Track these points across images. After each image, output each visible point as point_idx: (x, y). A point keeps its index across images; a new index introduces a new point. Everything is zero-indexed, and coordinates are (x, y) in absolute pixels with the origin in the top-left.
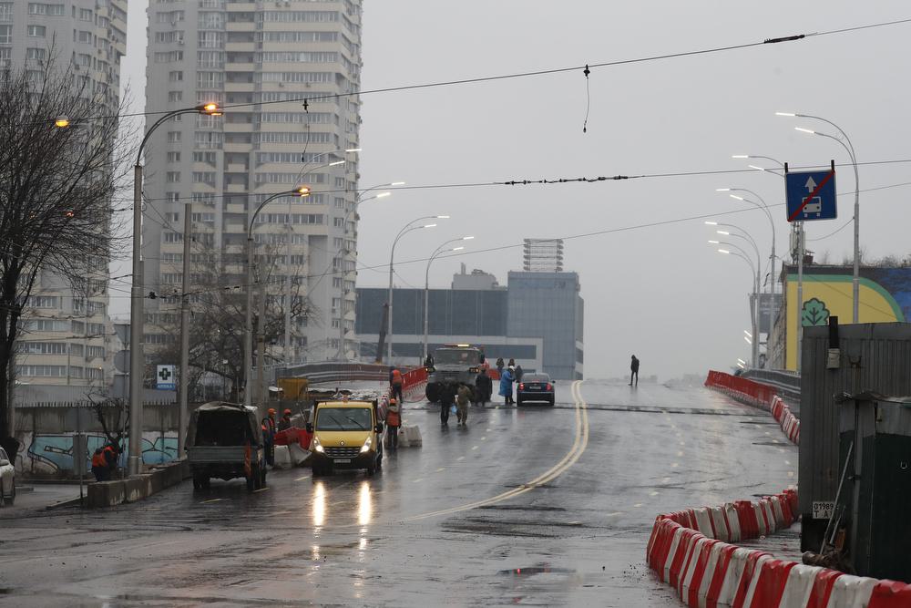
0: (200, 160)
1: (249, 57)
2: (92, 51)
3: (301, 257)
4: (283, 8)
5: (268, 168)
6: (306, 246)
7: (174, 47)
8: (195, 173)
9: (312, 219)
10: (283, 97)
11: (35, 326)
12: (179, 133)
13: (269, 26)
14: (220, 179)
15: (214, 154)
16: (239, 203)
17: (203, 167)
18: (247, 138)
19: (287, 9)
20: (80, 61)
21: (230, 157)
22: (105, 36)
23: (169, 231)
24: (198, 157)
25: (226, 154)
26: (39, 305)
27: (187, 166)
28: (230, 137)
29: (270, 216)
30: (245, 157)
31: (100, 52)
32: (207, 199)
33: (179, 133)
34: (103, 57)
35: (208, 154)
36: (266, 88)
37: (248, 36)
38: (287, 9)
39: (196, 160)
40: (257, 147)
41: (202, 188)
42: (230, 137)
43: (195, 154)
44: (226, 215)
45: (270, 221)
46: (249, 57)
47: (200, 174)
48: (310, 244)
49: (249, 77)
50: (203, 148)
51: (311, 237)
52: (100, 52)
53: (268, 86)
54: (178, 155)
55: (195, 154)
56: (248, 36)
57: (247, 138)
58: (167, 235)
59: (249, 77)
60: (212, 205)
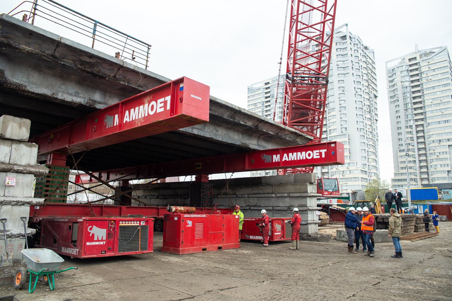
0: (408, 128)
1: (420, 97)
2: (361, 87)
3: (446, 152)
4: (429, 81)
5: (430, 127)
6: (448, 148)
7: (396, 99)
8: (406, 132)
9: (448, 140)
10: (433, 106)
11: (348, 172)
12: (400, 122)
13: (425, 87)
14: (414, 133)
15: (412, 126)
16: (422, 133)
17: (409, 130)
18: (422, 119)
19: (431, 80)
20: (357, 90)
21: (417, 126)
22: (367, 85)
23: (400, 149)
24: (407, 127)
25: (416, 125)
26: (349, 165)
27: (404, 130)
28: (416, 120)
29: (433, 141)
30: (422, 125)
31: (365, 90)
32: (412, 139)
33: (400, 122)
34: (367, 91)
35: (410, 126)
36: (426, 104)
37: (419, 91)
38: (431, 80)
39: (406, 128)
40: (426, 121)
41: (410, 136)
42: (416, 120)
43: (406, 127)
44: (418, 143)
45: (433, 142)
46: (420, 97)
47: (408, 132)
48: (449, 148)
49: (420, 102)
50: (408, 125)
51: (449, 146)
52: (365, 90)
53: (427, 103)
54: (401, 127)
55: (406, 127)
56: (419, 91)
57: (422, 119)
58: (400, 150)
59: (420, 102)
60: (413, 140)
